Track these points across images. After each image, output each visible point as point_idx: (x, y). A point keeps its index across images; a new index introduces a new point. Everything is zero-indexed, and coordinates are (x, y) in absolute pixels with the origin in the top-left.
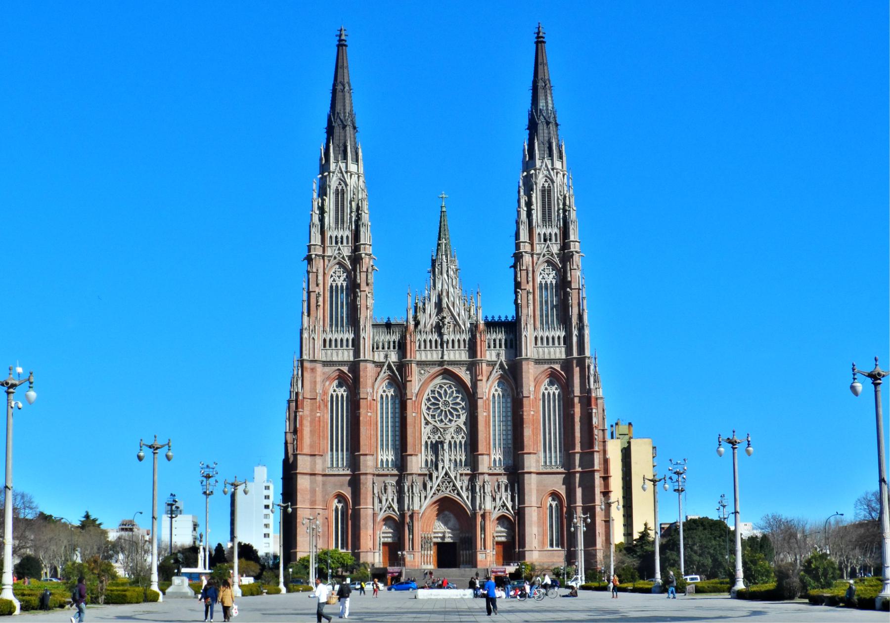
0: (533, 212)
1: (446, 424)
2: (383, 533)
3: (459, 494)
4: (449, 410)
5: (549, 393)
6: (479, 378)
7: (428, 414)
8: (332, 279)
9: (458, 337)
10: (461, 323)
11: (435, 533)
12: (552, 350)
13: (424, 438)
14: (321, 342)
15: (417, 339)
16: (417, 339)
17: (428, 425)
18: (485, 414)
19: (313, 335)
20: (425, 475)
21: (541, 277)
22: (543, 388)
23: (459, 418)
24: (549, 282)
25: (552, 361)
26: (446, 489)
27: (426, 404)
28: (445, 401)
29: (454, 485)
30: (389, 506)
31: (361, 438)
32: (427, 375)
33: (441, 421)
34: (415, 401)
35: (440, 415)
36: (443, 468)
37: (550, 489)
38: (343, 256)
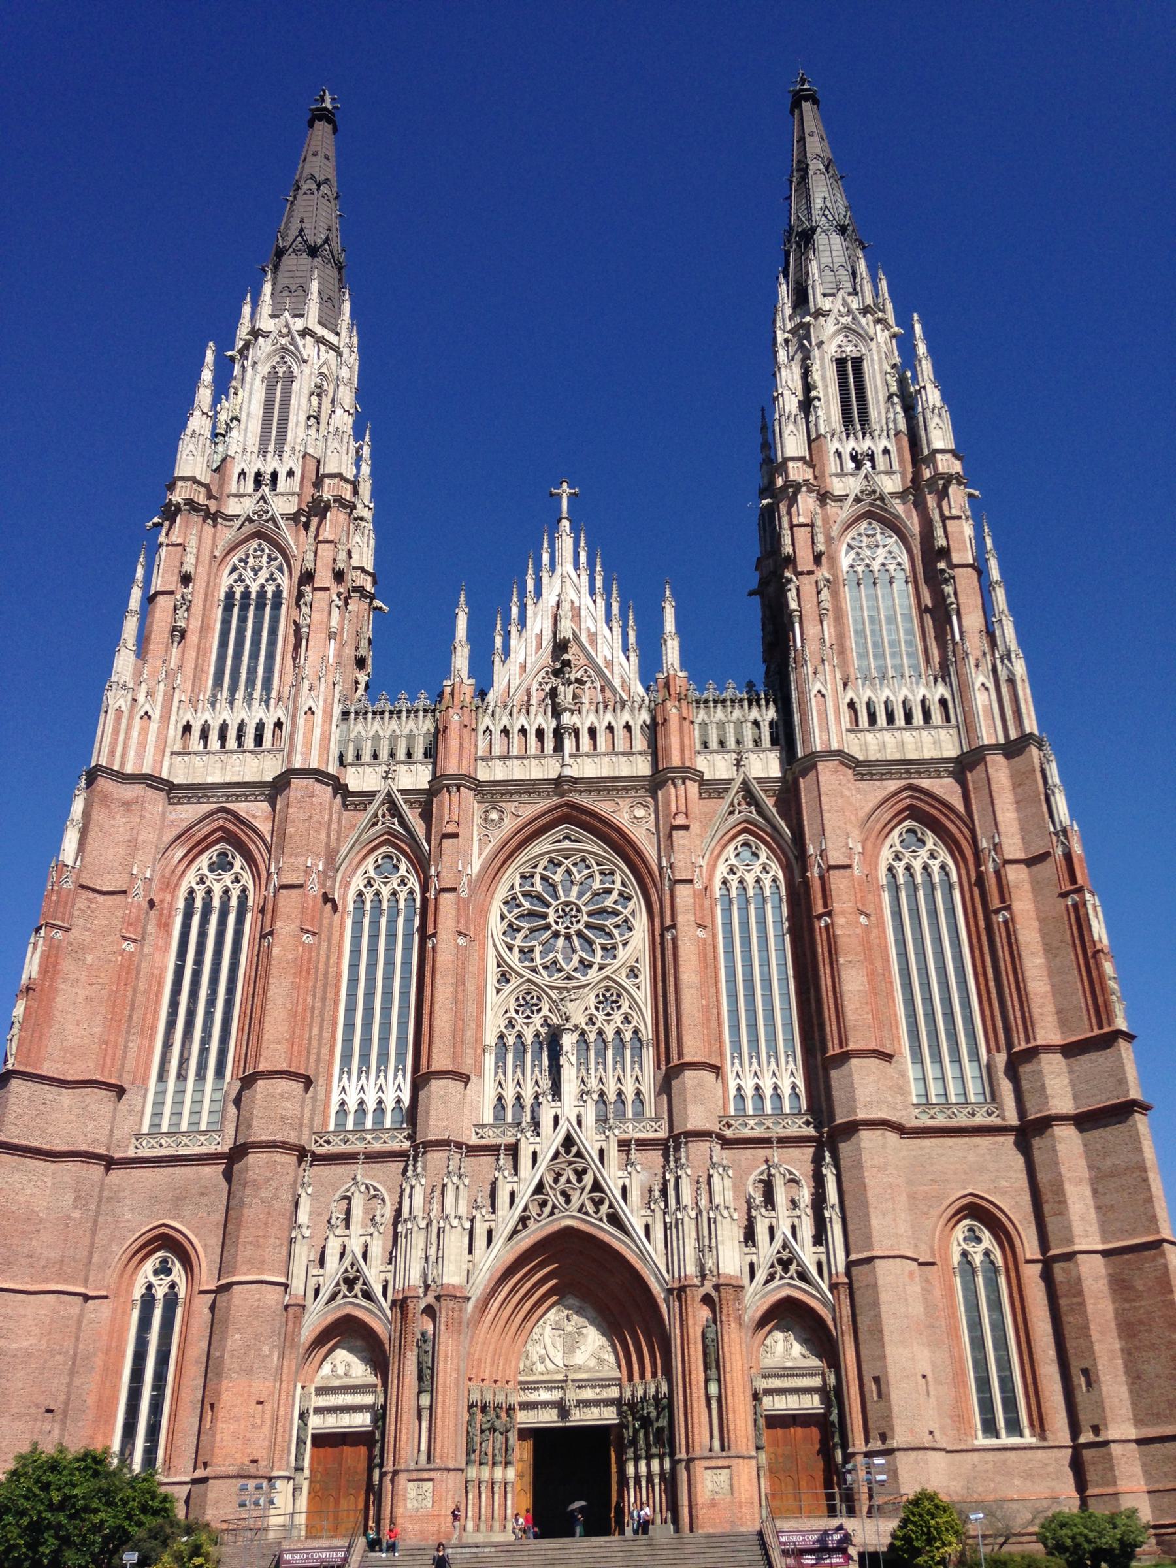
0: (816, 403)
1: (569, 978)
2: (322, 1391)
3: (614, 1219)
4: (579, 934)
5: (908, 868)
6: (681, 820)
7: (510, 949)
8: (235, 576)
9: (609, 717)
10: (617, 683)
11: (526, 1386)
12: (907, 736)
13: (493, 1025)
14: (174, 732)
15: (482, 728)
16: (482, 728)
17: (508, 981)
18: (701, 933)
19: (147, 707)
20: (494, 1150)
21: (852, 555)
22: (886, 855)
23: (615, 957)
24: (876, 566)
25: (913, 768)
26: (568, 1201)
27: (503, 917)
28: (567, 904)
29: (597, 1186)
30: (352, 1274)
31: (267, 1018)
32: (509, 825)
33: (553, 967)
34: (467, 901)
35: (547, 948)
36: (556, 1119)
37: (956, 1193)
38: (273, 519)
